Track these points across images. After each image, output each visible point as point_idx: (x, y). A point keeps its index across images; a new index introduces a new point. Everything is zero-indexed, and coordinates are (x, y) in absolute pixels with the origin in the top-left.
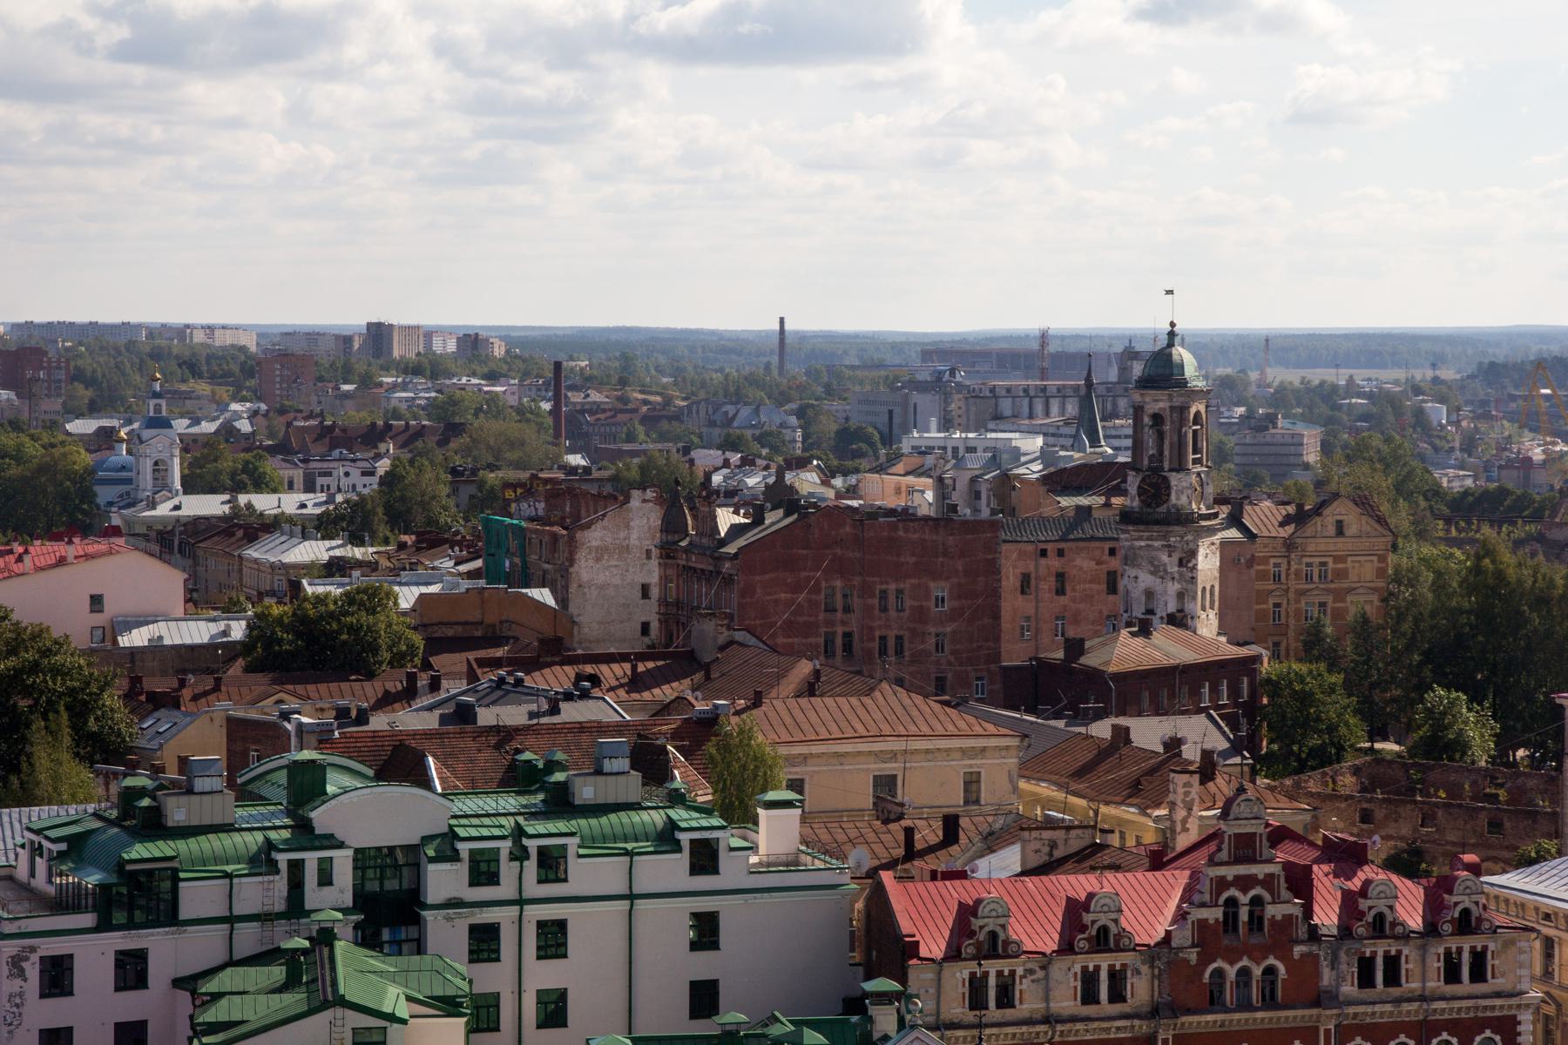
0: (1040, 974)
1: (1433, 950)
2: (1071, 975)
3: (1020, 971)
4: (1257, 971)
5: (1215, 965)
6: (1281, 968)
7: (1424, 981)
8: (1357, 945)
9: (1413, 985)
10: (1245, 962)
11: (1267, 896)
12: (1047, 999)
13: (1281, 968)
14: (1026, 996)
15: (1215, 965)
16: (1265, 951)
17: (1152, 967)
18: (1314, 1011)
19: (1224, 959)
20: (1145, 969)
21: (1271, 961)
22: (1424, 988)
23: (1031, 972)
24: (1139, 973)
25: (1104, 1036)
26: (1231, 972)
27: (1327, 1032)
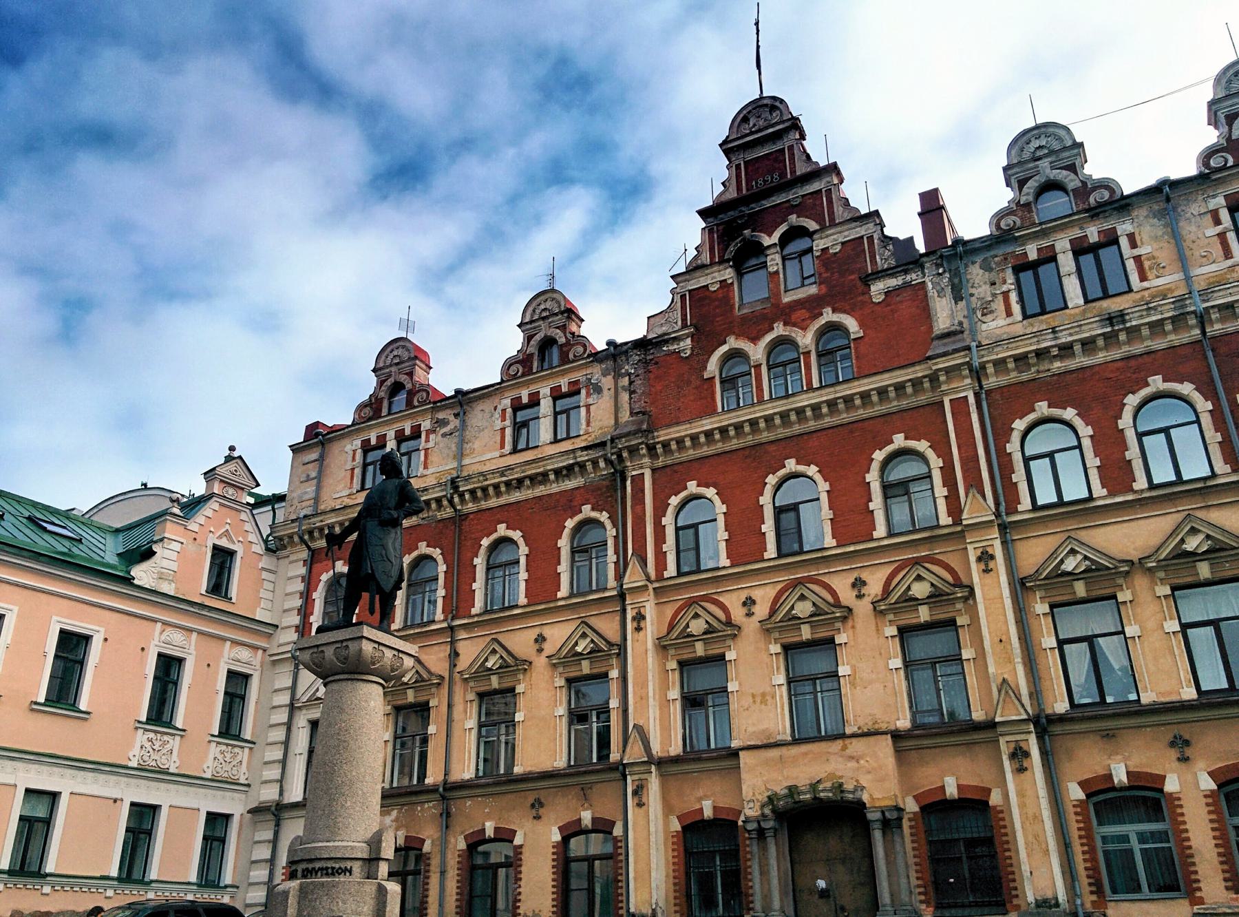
0: (454, 423)
1: (1195, 208)
2: (497, 415)
3: (426, 425)
4: (806, 339)
5: (724, 349)
6: (851, 324)
7: (1183, 262)
8: (1010, 249)
9: (1156, 283)
10: (779, 330)
11: (812, 225)
12: (460, 455)
13: (851, 324)
14: (433, 458)
15: (724, 349)
16: (812, 306)
17: (618, 376)
18: (919, 371)
19: (738, 336)
20: (607, 382)
21: (828, 316)
22: (1188, 279)
23: (443, 423)
24: (598, 390)
25: (540, 490)
26: (757, 352)
27: (960, 406)
